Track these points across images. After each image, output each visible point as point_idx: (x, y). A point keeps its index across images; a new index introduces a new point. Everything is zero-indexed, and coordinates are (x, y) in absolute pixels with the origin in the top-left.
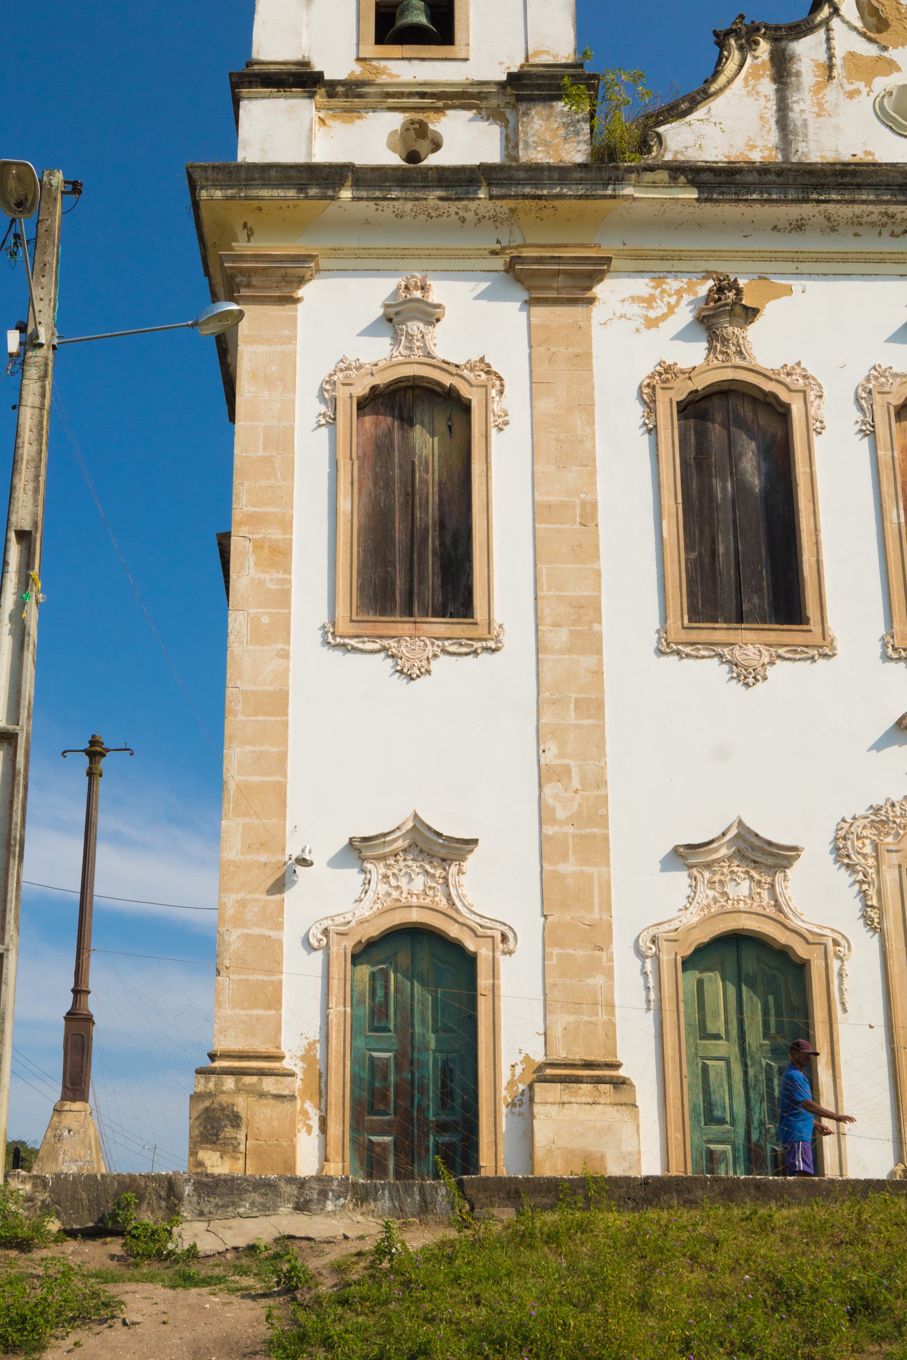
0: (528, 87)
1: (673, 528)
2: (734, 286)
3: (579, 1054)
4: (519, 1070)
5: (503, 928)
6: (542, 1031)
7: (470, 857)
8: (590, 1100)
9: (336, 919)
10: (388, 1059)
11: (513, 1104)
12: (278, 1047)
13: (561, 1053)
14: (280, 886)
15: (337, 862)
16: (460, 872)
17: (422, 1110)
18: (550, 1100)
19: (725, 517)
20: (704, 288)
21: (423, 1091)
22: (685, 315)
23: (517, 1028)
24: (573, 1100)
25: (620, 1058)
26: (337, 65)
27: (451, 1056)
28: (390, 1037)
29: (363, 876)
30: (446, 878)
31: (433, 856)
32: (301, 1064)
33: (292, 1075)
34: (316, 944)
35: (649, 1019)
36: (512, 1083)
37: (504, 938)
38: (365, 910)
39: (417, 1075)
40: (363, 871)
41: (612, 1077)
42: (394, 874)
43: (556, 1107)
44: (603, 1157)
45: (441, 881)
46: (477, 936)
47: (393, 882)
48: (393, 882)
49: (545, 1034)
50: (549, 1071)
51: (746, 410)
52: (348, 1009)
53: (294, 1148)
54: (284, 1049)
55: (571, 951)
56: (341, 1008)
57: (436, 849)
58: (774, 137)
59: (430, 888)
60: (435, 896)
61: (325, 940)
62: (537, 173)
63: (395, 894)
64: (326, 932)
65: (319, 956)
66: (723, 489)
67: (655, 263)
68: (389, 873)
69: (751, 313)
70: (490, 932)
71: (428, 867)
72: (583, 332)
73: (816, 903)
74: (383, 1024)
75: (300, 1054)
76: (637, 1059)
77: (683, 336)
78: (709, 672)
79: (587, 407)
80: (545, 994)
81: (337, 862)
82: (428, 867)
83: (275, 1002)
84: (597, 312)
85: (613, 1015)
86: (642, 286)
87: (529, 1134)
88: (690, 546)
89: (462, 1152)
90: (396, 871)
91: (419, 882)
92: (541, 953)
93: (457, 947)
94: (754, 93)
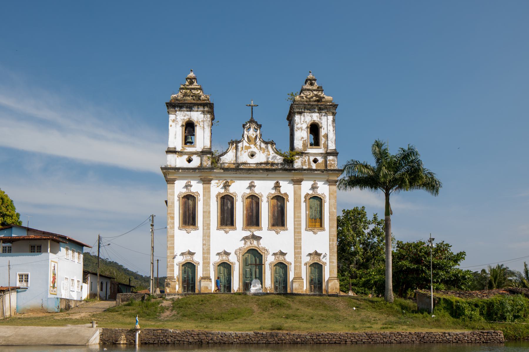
0: (203, 153)
1: (219, 214)
2: (228, 182)
19: (226, 211)
20: (224, 182)
22: (222, 185)
26: (179, 149)
51: (229, 198)
58: (235, 159)
62: (204, 169)
66: (226, 208)
67: (219, 178)
69: (230, 186)
72: (209, 188)
73: (233, 259)
77: (222, 188)
78: (223, 232)
79: (209, 198)
84: (212, 185)
86: (217, 181)
88: (221, 215)
89: (193, 289)
94: (233, 152)
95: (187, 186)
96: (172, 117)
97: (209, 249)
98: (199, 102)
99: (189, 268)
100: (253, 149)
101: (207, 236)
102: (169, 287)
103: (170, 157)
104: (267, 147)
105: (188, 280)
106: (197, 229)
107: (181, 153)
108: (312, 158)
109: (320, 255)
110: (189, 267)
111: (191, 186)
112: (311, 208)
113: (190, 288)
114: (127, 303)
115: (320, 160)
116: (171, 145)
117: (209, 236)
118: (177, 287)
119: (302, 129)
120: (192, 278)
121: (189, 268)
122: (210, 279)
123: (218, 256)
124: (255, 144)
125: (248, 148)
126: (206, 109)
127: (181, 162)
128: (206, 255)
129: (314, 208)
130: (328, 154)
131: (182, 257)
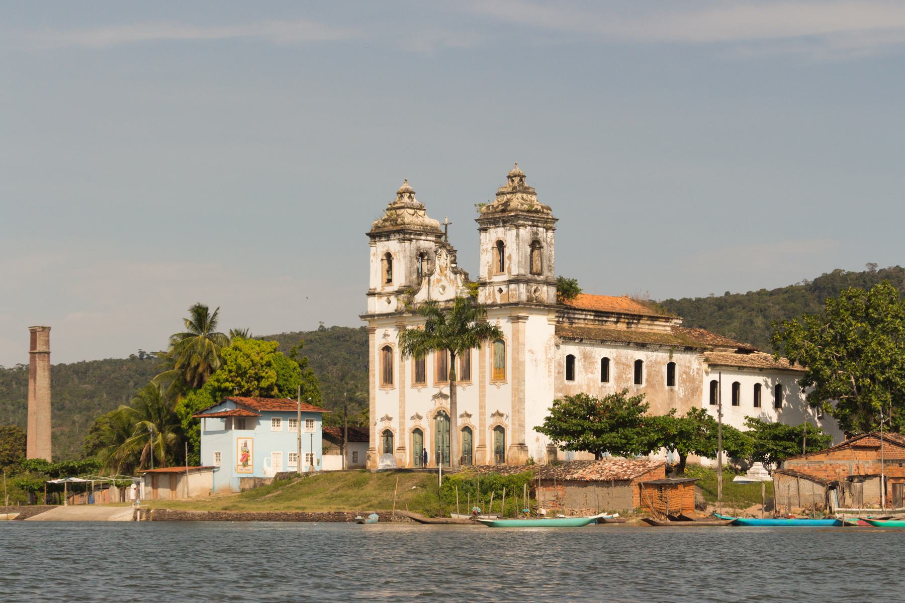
0: (398, 293)
95: (385, 335)
96: (373, 250)
97: (404, 413)
98: (395, 228)
100: (444, 282)
101: (402, 395)
103: (371, 300)
104: (456, 278)
106: (393, 388)
107: (380, 294)
108: (497, 288)
109: (502, 415)
111: (388, 335)
112: (495, 354)
115: (504, 288)
116: (372, 287)
117: (404, 397)
119: (487, 250)
124: (446, 276)
125: (439, 281)
126: (402, 236)
127: (377, 306)
129: (498, 355)
130: (510, 282)
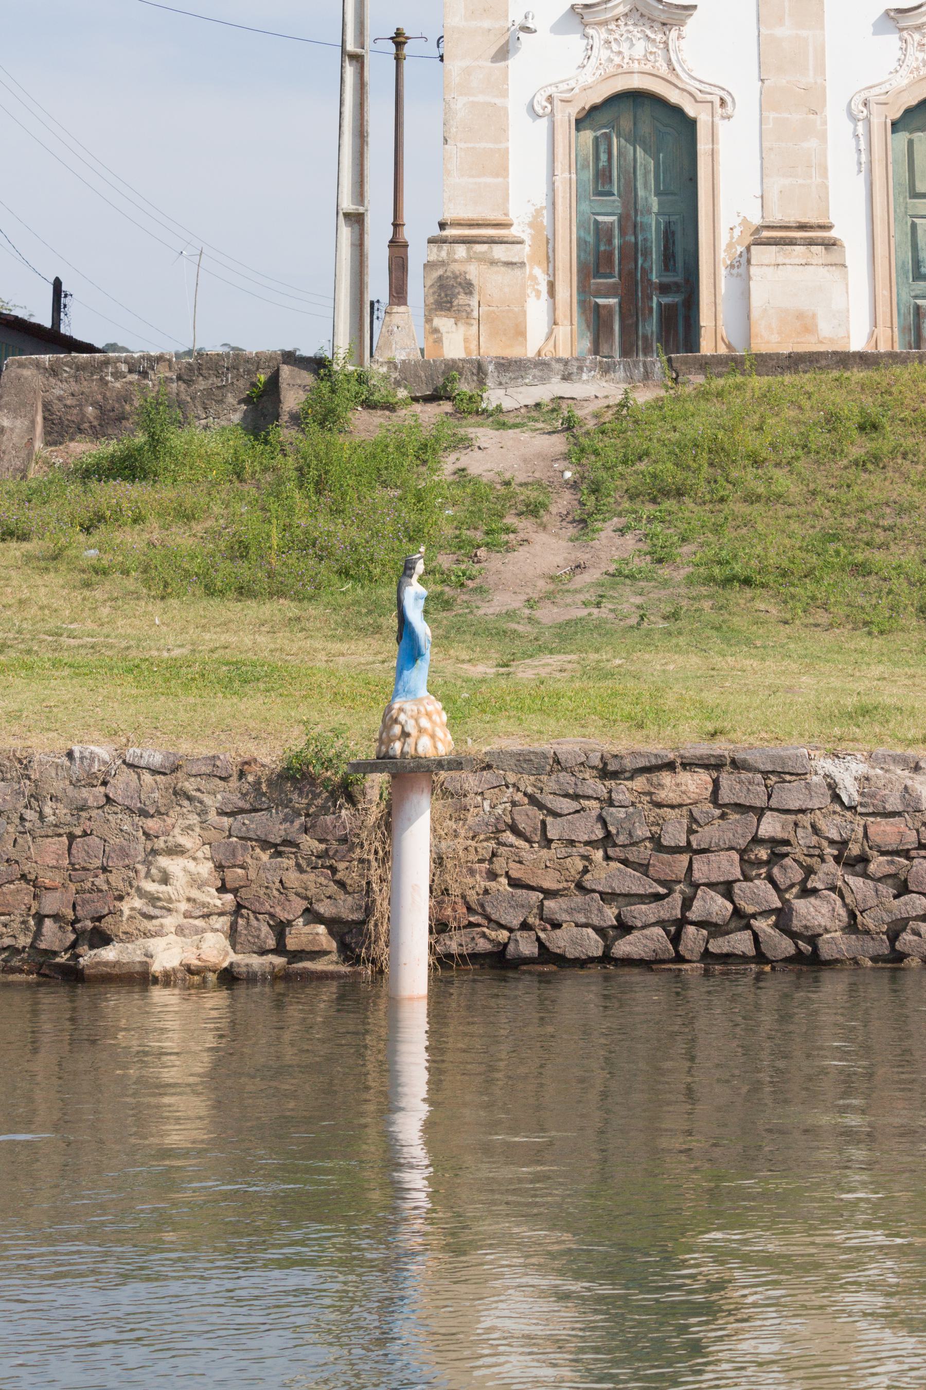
3: (793, 218)
4: (737, 232)
5: (722, 93)
6: (759, 194)
7: (690, 21)
8: (803, 262)
9: (560, 85)
10: (612, 223)
11: (732, 266)
12: (506, 215)
13: (777, 216)
14: (503, 53)
15: (559, 28)
16: (680, 37)
17: (646, 272)
18: (767, 262)
21: (646, 253)
23: (734, 194)
24: (787, 261)
25: (833, 220)
27: (673, 218)
28: (614, 201)
29: (585, 41)
30: (666, 43)
31: (654, 21)
32: (529, 231)
33: (521, 242)
34: (540, 112)
35: (860, 183)
36: (730, 246)
37: (723, 102)
38: (588, 77)
39: (640, 238)
40: (585, 36)
41: (823, 238)
42: (615, 39)
43: (772, 268)
44: (814, 316)
45: (662, 46)
46: (696, 101)
47: (615, 46)
48: (615, 46)
49: (762, 197)
50: (766, 234)
52: (574, 176)
53: (524, 313)
54: (513, 216)
55: (786, 115)
56: (567, 175)
57: (656, 13)
59: (651, 53)
60: (656, 61)
61: (549, 106)
63: (617, 60)
64: (550, 99)
65: (544, 123)
68: (611, 38)
70: (709, 98)
71: (648, 32)
74: (607, 188)
75: (527, 220)
76: (849, 223)
80: (762, 158)
81: (559, 28)
82: (648, 32)
83: (502, 170)
85: (827, 178)
87: (746, 295)
90: (617, 36)
91: (640, 47)
92: (758, 117)
93: (677, 111)
99: (645, 136)
102: (462, 315)
105: (631, 252)
110: (634, 139)
113: (651, 327)
114: (109, 448)
118: (536, 312)
120: (668, 236)
121: (645, 136)
122: (830, 244)
123: (893, 40)
128: (784, 31)
131: (575, 42)
